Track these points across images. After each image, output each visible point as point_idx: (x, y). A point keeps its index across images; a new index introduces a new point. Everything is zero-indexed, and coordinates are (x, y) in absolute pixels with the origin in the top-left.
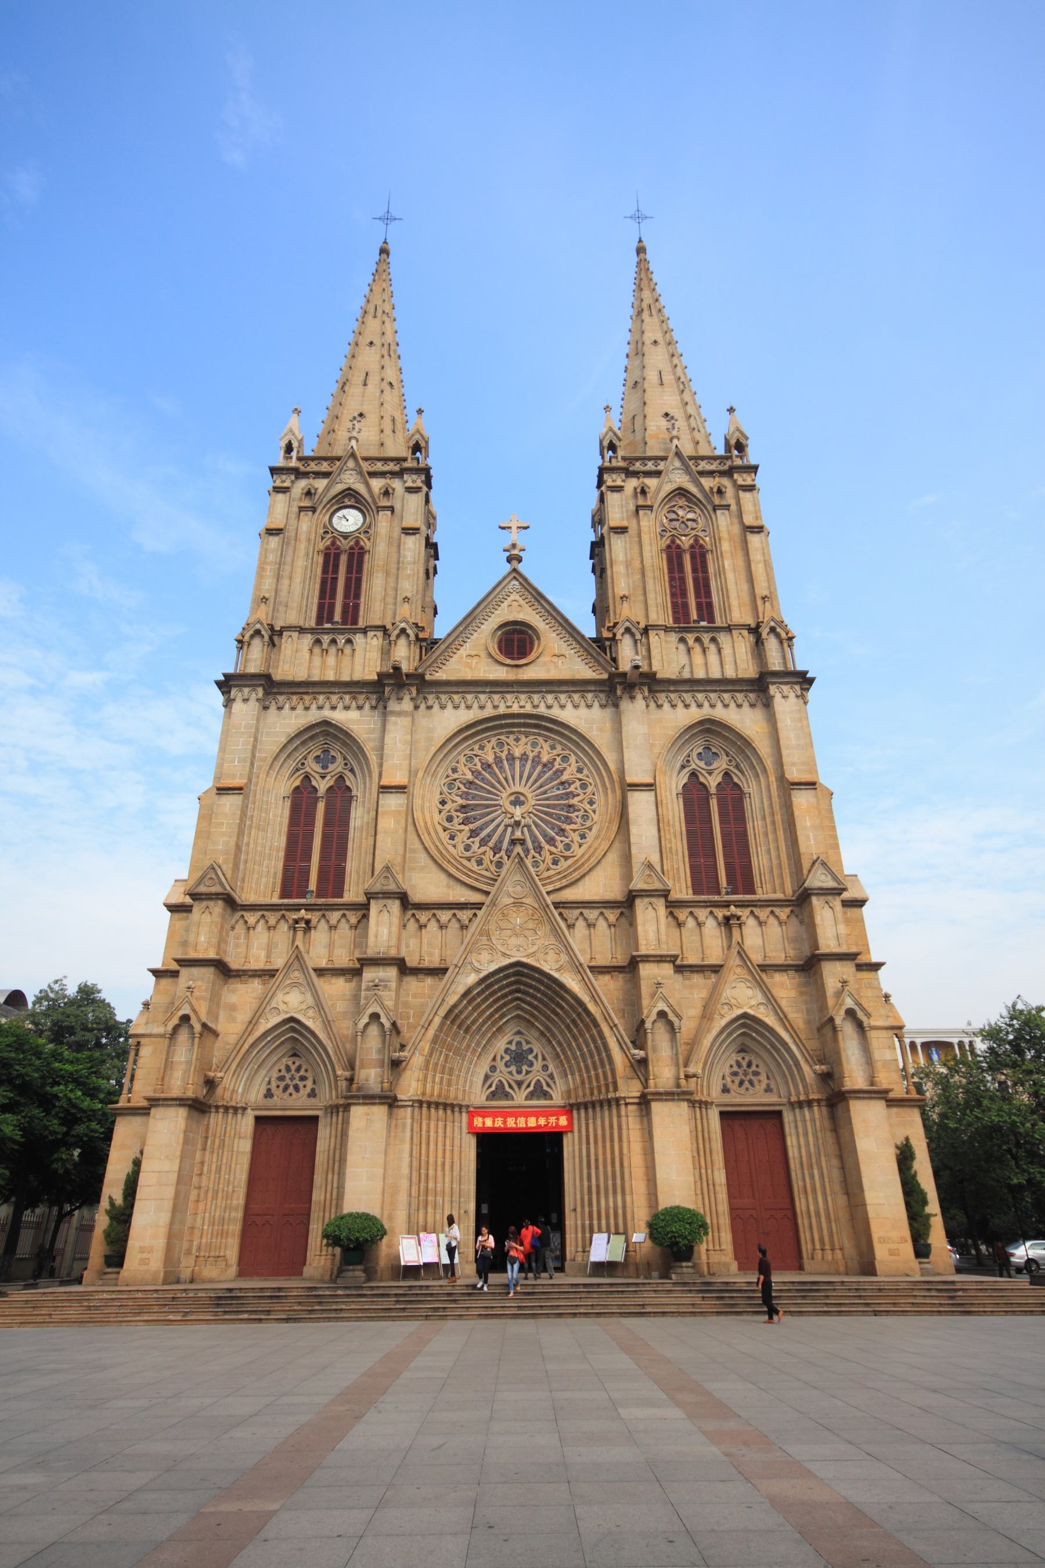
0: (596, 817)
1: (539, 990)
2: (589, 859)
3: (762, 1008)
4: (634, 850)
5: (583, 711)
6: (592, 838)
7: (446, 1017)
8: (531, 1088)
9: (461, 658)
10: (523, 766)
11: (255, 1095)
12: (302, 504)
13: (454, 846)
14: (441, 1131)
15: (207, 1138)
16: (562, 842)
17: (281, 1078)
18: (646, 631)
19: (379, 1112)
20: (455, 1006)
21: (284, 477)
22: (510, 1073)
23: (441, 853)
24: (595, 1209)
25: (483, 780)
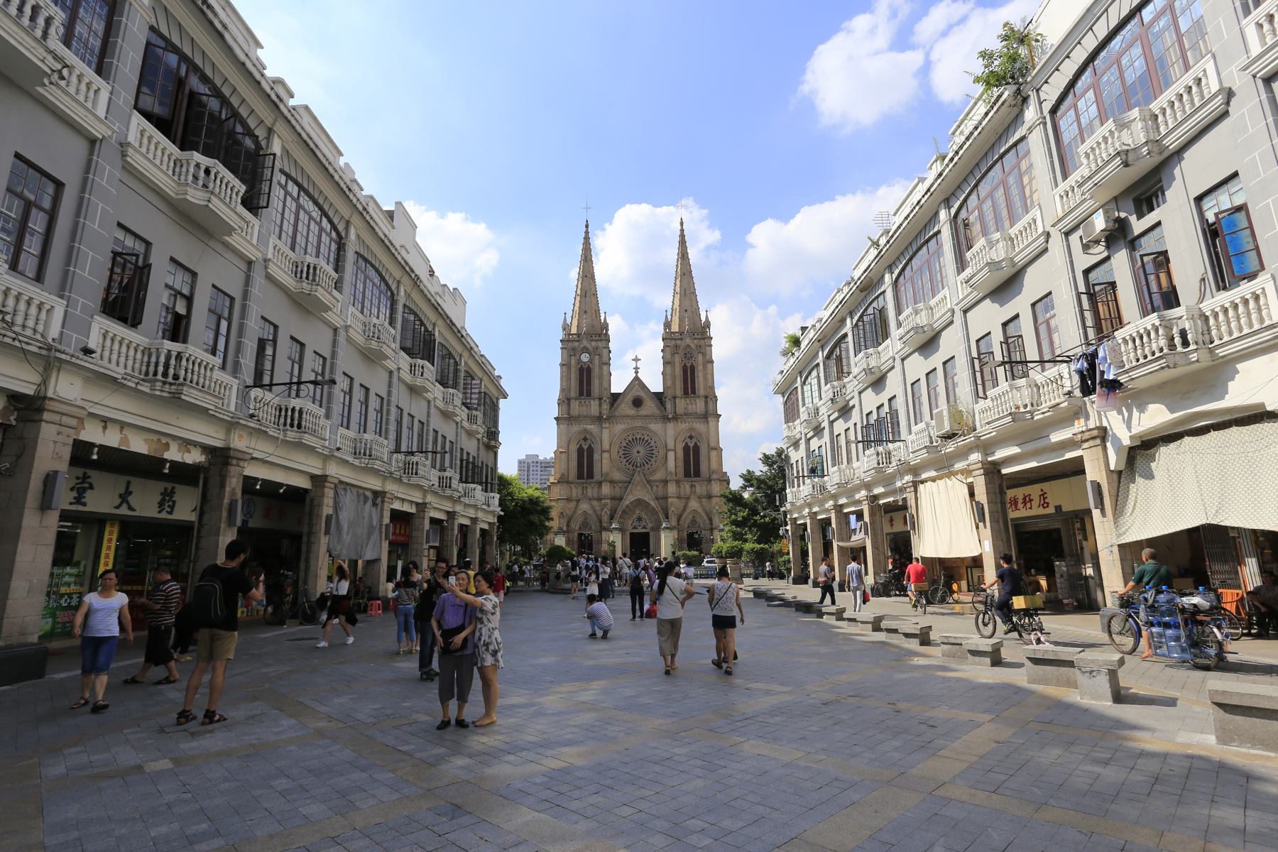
11: (577, 528)
18: (675, 398)
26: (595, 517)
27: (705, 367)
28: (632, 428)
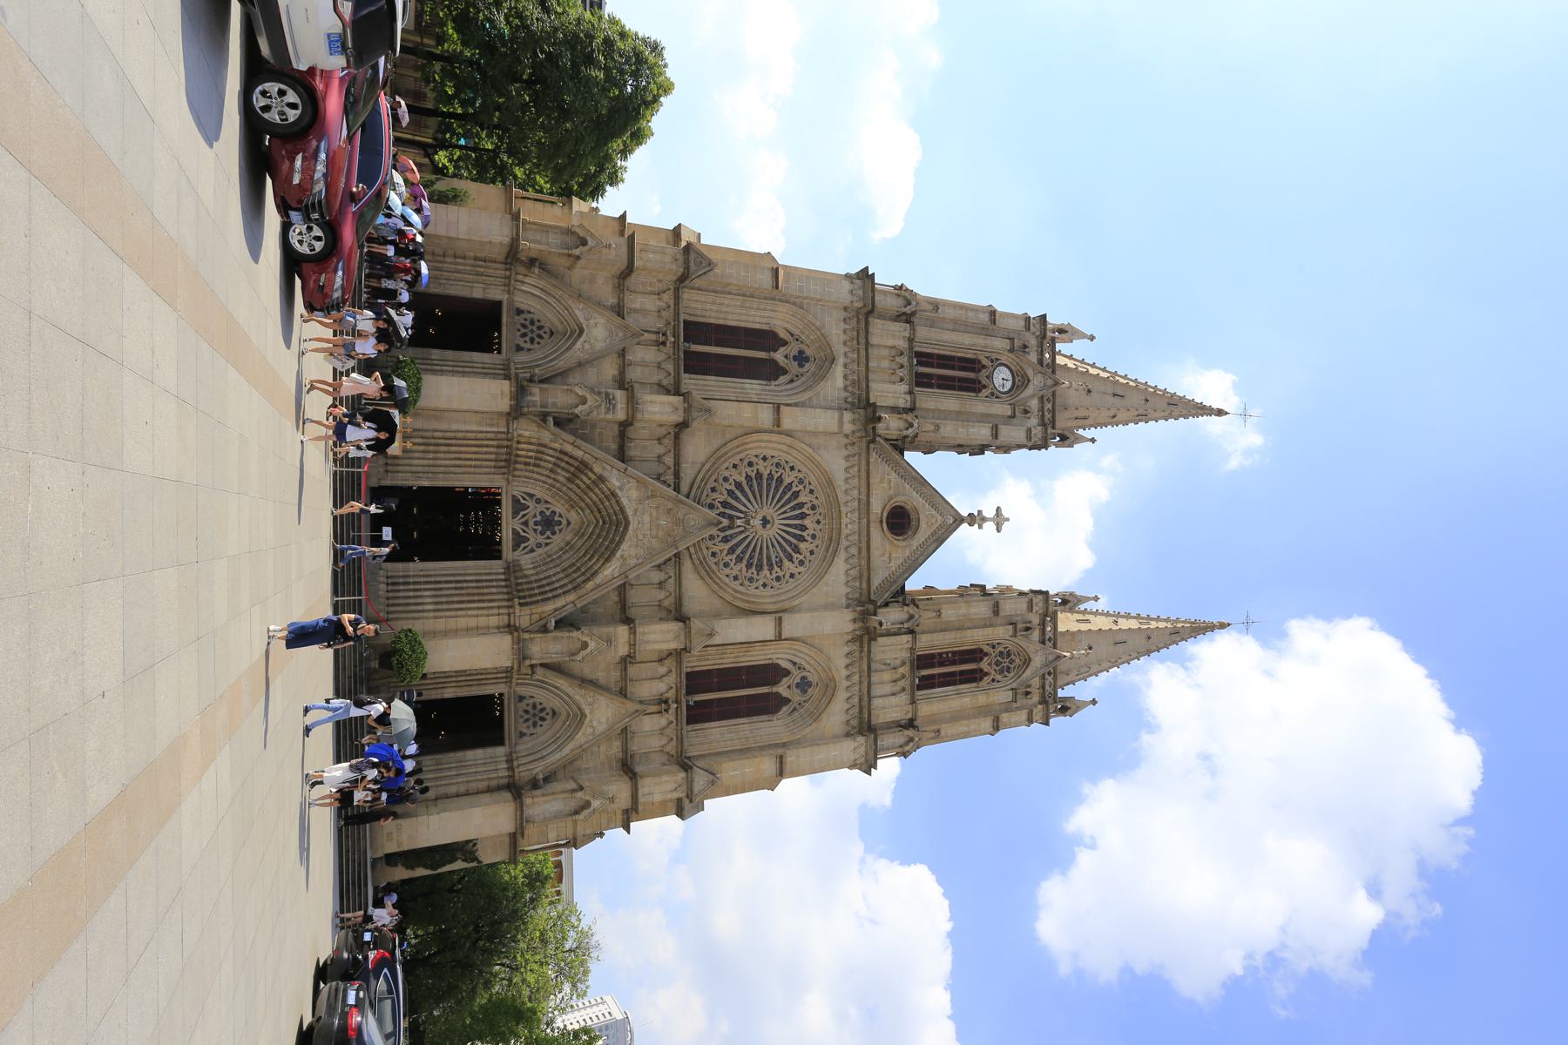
0: (752, 591)
1: (605, 540)
2: (716, 583)
3: (590, 730)
4: (724, 622)
5: (843, 578)
6: (735, 587)
7: (582, 462)
8: (522, 534)
9: (889, 475)
10: (796, 527)
11: (521, 301)
12: (1016, 341)
13: (727, 468)
14: (488, 456)
15: (485, 261)
16: (731, 560)
17: (532, 323)
18: (911, 632)
19: (504, 404)
20: (591, 470)
21: (1038, 326)
22: (535, 516)
23: (721, 457)
24: (423, 587)
25: (784, 493)
26: (561, 364)
27: (982, 711)
28: (833, 503)
